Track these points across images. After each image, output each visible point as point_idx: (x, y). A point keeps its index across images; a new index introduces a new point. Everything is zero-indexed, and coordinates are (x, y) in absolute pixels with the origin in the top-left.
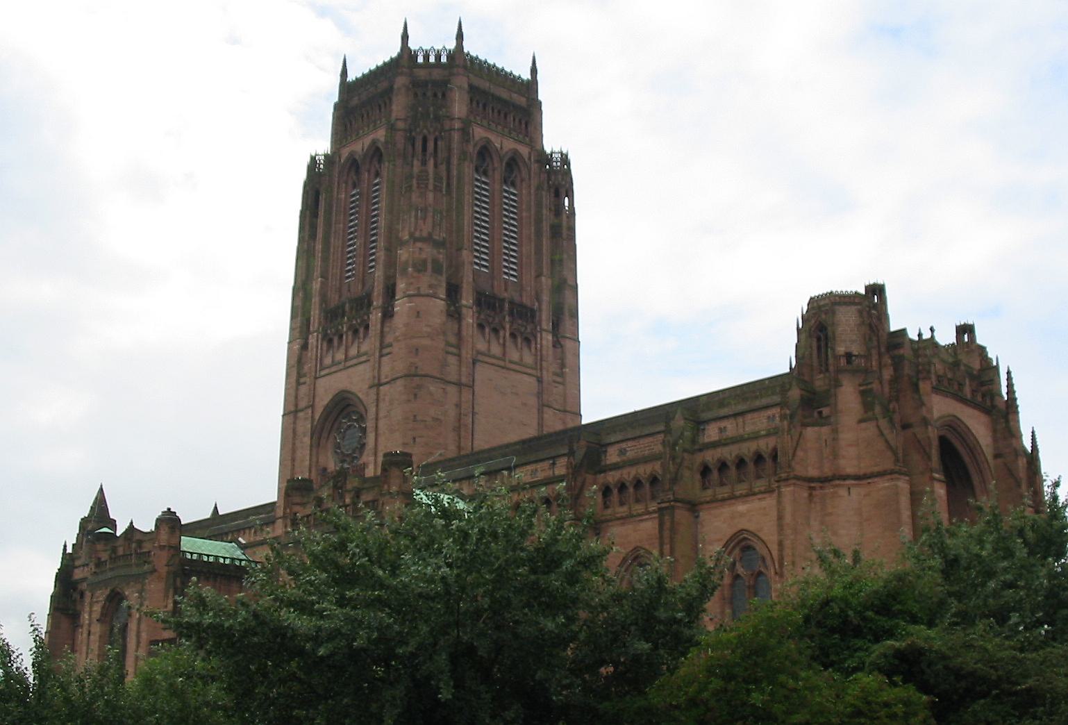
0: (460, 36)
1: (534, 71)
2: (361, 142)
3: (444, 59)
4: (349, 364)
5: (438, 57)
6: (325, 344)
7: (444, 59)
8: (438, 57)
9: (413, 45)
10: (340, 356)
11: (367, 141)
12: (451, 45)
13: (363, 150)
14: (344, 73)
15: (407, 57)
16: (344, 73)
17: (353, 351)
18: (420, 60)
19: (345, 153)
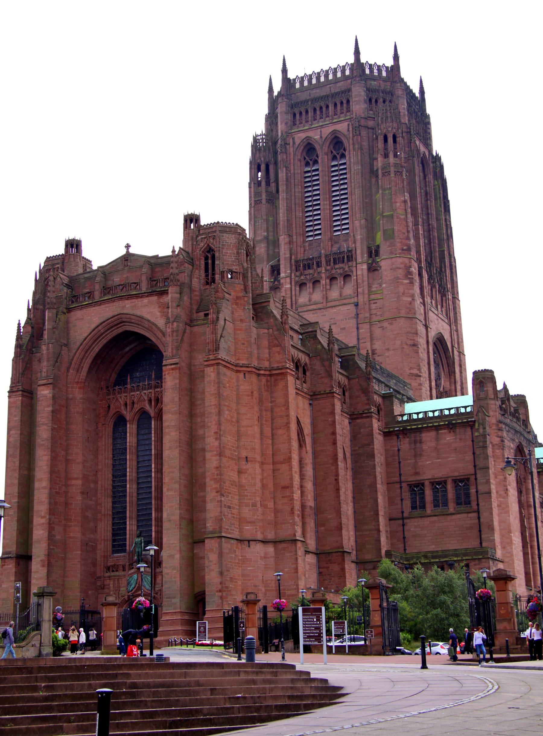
0: (396, 57)
2: (319, 130)
3: (384, 74)
4: (330, 304)
6: (298, 288)
7: (384, 74)
9: (363, 60)
10: (317, 296)
11: (327, 131)
12: (390, 63)
13: (321, 137)
14: (284, 71)
16: (284, 71)
17: (334, 294)
18: (367, 71)
19: (300, 137)
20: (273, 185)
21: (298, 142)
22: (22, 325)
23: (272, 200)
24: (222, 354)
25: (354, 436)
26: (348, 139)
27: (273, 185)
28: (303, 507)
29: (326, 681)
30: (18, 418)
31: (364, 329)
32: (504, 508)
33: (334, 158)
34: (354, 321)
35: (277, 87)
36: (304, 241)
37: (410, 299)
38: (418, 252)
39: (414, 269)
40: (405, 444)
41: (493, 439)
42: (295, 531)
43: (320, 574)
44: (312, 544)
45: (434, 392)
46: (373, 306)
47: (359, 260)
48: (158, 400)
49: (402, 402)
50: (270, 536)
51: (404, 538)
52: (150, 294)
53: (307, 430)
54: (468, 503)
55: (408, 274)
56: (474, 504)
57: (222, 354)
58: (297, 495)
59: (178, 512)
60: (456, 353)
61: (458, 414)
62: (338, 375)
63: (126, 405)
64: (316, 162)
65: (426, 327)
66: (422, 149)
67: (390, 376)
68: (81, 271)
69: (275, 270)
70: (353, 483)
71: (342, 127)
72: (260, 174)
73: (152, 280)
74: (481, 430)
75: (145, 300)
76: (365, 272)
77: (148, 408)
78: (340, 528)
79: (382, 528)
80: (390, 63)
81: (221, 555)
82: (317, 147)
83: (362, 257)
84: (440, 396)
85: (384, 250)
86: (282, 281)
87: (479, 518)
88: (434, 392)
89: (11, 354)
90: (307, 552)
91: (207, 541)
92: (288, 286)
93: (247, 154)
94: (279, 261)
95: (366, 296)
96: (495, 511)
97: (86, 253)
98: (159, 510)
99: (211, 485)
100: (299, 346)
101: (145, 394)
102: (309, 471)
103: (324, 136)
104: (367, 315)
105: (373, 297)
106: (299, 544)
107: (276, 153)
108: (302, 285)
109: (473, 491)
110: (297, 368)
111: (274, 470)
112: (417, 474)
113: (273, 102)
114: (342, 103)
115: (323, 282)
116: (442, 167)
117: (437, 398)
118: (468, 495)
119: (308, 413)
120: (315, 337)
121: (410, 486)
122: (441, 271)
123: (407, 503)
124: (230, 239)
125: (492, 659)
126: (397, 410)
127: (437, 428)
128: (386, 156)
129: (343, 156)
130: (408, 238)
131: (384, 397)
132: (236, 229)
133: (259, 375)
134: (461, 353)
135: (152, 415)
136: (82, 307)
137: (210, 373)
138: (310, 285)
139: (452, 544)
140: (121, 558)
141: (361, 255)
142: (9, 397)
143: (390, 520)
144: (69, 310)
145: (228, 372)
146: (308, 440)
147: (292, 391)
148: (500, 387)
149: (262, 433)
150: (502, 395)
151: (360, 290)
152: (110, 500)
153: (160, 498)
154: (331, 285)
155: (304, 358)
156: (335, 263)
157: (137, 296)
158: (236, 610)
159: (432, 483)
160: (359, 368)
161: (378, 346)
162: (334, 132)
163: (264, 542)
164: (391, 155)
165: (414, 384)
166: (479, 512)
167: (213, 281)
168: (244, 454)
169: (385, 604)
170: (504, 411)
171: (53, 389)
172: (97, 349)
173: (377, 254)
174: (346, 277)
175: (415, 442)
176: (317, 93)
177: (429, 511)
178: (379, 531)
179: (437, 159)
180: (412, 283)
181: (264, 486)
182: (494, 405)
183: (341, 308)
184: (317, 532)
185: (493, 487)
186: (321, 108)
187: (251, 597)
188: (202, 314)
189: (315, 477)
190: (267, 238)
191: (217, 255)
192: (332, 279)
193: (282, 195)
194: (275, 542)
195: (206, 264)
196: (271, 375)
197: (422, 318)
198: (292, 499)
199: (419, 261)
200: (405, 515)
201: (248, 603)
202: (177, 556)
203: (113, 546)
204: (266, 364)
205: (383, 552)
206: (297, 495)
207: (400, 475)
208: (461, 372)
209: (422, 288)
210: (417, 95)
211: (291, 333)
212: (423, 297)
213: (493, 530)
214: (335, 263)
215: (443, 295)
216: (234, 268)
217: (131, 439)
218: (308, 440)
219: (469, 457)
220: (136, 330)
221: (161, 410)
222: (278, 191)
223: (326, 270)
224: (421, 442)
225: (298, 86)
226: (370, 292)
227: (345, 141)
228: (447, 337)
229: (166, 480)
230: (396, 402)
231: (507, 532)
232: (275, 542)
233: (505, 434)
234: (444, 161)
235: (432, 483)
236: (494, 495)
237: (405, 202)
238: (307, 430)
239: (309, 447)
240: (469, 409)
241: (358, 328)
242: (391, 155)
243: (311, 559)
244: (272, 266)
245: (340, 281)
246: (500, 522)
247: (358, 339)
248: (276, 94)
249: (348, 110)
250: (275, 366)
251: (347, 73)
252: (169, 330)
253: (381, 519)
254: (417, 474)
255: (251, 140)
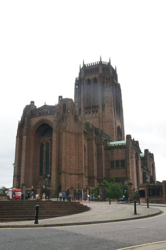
0: (110, 60)
1: (116, 68)
3: (107, 64)
5: (106, 63)
7: (107, 64)
8: (106, 63)
9: (102, 61)
10: (90, 116)
11: (93, 77)
14: (84, 63)
15: (101, 62)
16: (84, 63)
17: (94, 115)
18: (103, 63)
19: (87, 78)
20: (80, 89)
21: (86, 79)
22: (20, 121)
23: (80, 93)
24: (67, 129)
25: (98, 150)
26: (98, 79)
27: (80, 89)
28: (85, 166)
29: (87, 206)
30: (18, 143)
31: (101, 124)
32: (132, 168)
33: (95, 83)
34: (98, 122)
35: (82, 66)
36: (87, 103)
37: (111, 117)
38: (114, 106)
39: (113, 110)
40: (110, 152)
41: (130, 151)
42: (83, 172)
43: (88, 182)
44: (87, 175)
45: (117, 139)
46: (103, 119)
47: (100, 107)
48: (51, 140)
49: (109, 142)
50: (77, 173)
51: (109, 174)
52: (50, 114)
53: (86, 148)
54: (124, 166)
55: (112, 111)
56: (125, 166)
57: (67, 129)
58: (84, 164)
59: (55, 167)
60: (122, 130)
61: (122, 145)
62: (94, 135)
63: (44, 141)
64: (90, 84)
65: (116, 124)
66: (116, 82)
67: (106, 135)
68: (34, 109)
69: (80, 109)
70: (97, 161)
71: (97, 76)
72: (77, 86)
73: (51, 111)
74: (128, 149)
75: (49, 116)
76: (101, 110)
77: (49, 142)
78: (94, 171)
79: (104, 172)
80: (108, 62)
81: (65, 178)
82: (91, 80)
83: (101, 106)
84: (118, 141)
85: (106, 106)
86: (82, 112)
87: (126, 170)
88: (117, 139)
89: (17, 128)
90: (86, 177)
91: (62, 174)
92: (83, 113)
93: (74, 82)
94: (81, 107)
95: (101, 116)
96: (130, 168)
97: (35, 104)
98: (51, 166)
99: (63, 160)
100: (85, 128)
101: (48, 138)
102: (87, 158)
103: (93, 78)
104: (102, 121)
105: (103, 116)
106: (84, 175)
107: (81, 81)
108: (86, 113)
109: (125, 163)
110: (84, 133)
111: (78, 157)
112: (112, 159)
113: (81, 70)
114: (97, 70)
115: (91, 112)
116: (120, 86)
117: (118, 141)
118: (124, 164)
119: (87, 144)
120: (89, 126)
121: (111, 162)
122: (119, 110)
123: (110, 166)
124: (70, 102)
125: (127, 203)
126: (108, 144)
127: (118, 148)
128: (107, 83)
129: (97, 83)
130: (112, 103)
131: (105, 140)
132: (71, 100)
133: (75, 134)
134: (124, 130)
135: (50, 143)
136: (34, 117)
137: (64, 134)
138: (88, 113)
139: (120, 176)
140: (42, 177)
141: (100, 106)
142: (16, 138)
143: (106, 170)
144: (31, 118)
145: (68, 134)
146: (87, 150)
147: (83, 138)
148: (132, 139)
149: (76, 149)
150: (133, 141)
151: (100, 115)
152: (39, 163)
153: (51, 163)
154: (93, 113)
155: (86, 131)
156: (94, 108)
157: (47, 115)
158: (68, 190)
159: (116, 161)
160: (99, 133)
161: (104, 128)
162: (95, 77)
163: (76, 174)
164: (108, 83)
165: (112, 137)
166: (126, 168)
167: (65, 111)
168: (71, 153)
169: (103, 190)
170: (133, 144)
171: (27, 136)
172: (37, 127)
173: (104, 106)
174: (97, 111)
175: (112, 151)
176: (92, 68)
177: (115, 168)
178: (103, 172)
179: (119, 84)
180: (112, 113)
181: (76, 161)
182: (131, 143)
183: (96, 119)
184: (88, 172)
185: (130, 162)
186: (92, 71)
187: (72, 187)
188: (62, 120)
189: (88, 159)
190: (78, 102)
191: (66, 106)
192: (94, 112)
193: (82, 92)
194: (78, 174)
195: (64, 108)
196: (78, 135)
197: (115, 122)
198: (82, 164)
199: (114, 108)
200: (109, 169)
201: (72, 189)
202: (55, 177)
203: (40, 174)
204: (77, 132)
205: (104, 177)
206: (84, 164)
207: (108, 159)
208: (123, 135)
209: (115, 115)
210: (115, 69)
211: (83, 125)
212: (115, 117)
213: (130, 172)
214: (94, 108)
215: (120, 116)
216: (71, 109)
217: (45, 149)
218: (87, 150)
219: (125, 155)
220: (46, 123)
221: (52, 142)
222: (81, 91)
223: (92, 110)
224: (113, 151)
225: (87, 66)
226: (102, 115)
227: (97, 79)
228: (120, 126)
229: (53, 159)
230: (108, 142)
231: (133, 173)
232: (78, 174)
233: (133, 150)
234: (121, 85)
235: (116, 161)
236: (130, 164)
237: (111, 94)
238: (86, 148)
239: (87, 152)
240: (125, 144)
241: (99, 124)
242: (108, 83)
243: (87, 179)
244: (79, 108)
245: (95, 112)
246: (132, 171)
247: (99, 126)
248: (81, 68)
249: (98, 72)
250: (79, 132)
251: (98, 63)
252: (54, 123)
253: (103, 169)
254: (112, 159)
255: (75, 79)
